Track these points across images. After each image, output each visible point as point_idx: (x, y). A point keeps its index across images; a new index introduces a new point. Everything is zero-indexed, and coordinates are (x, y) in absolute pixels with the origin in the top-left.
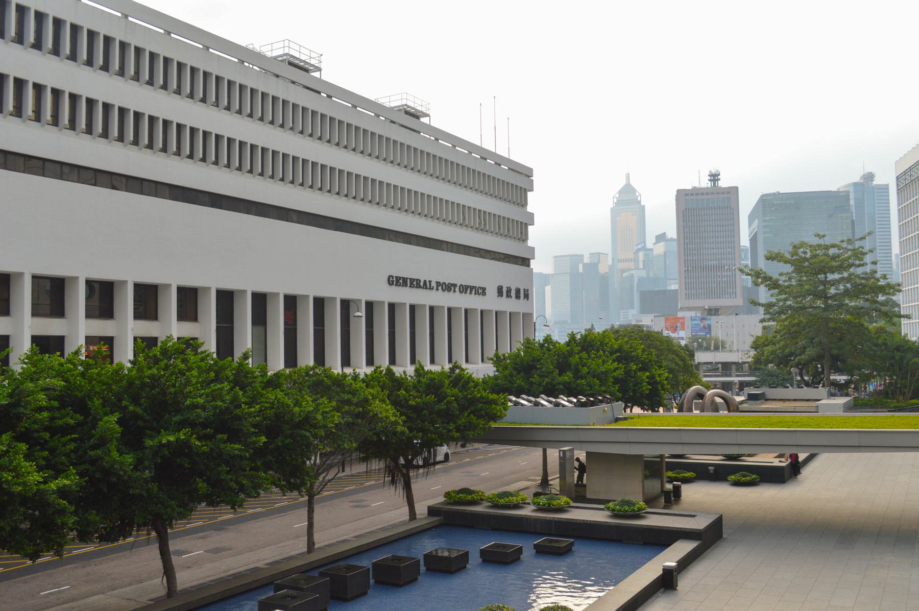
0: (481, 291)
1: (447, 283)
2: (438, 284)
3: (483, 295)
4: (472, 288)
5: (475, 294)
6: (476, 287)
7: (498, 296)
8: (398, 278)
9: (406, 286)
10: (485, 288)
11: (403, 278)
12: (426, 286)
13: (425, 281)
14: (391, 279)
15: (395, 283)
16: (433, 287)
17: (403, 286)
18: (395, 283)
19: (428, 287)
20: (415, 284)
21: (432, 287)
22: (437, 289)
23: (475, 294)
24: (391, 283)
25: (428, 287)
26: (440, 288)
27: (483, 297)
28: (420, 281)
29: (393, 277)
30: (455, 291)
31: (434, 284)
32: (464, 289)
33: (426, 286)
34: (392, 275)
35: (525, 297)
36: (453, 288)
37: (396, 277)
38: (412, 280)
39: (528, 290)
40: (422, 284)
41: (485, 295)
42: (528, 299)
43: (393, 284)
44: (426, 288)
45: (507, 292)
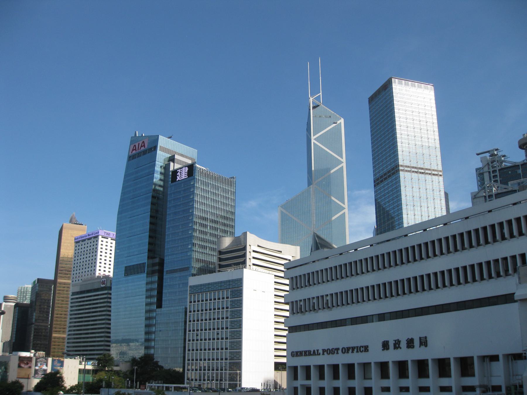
0: (364, 349)
1: (331, 349)
2: (324, 351)
3: (365, 351)
4: (353, 349)
5: (357, 352)
6: (357, 347)
7: (383, 350)
8: (297, 352)
9: (302, 355)
10: (368, 346)
11: (300, 352)
12: (315, 353)
13: (314, 351)
14: (293, 353)
15: (295, 355)
16: (320, 353)
17: (300, 356)
18: (295, 355)
19: (316, 354)
20: (307, 353)
21: (319, 354)
22: (323, 354)
23: (357, 352)
24: (293, 355)
25: (316, 354)
26: (325, 353)
27: (366, 353)
28: (311, 351)
29: (294, 352)
30: (337, 353)
31: (321, 351)
32: (346, 350)
33: (315, 353)
34: (293, 351)
35: (421, 344)
36: (336, 352)
37: (296, 352)
38: (305, 352)
39: (426, 337)
40: (312, 353)
41: (368, 351)
42: (426, 346)
43: (294, 356)
44: (315, 355)
45: (395, 345)
